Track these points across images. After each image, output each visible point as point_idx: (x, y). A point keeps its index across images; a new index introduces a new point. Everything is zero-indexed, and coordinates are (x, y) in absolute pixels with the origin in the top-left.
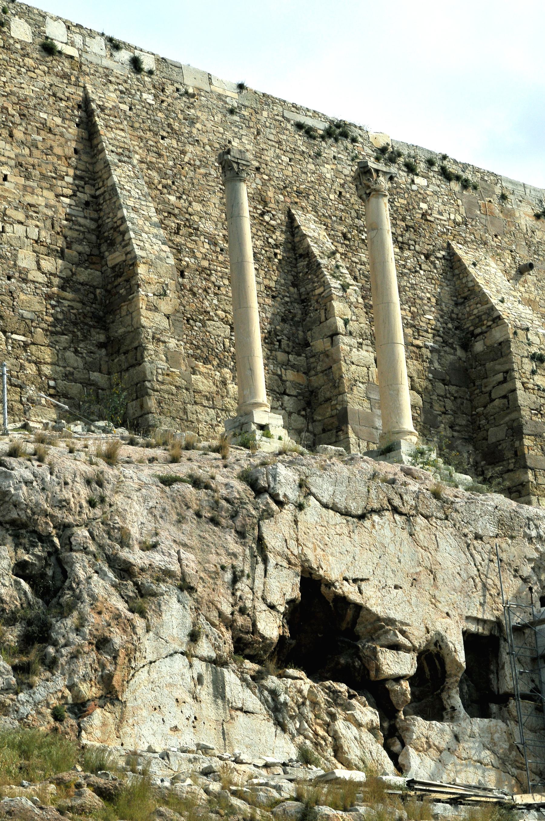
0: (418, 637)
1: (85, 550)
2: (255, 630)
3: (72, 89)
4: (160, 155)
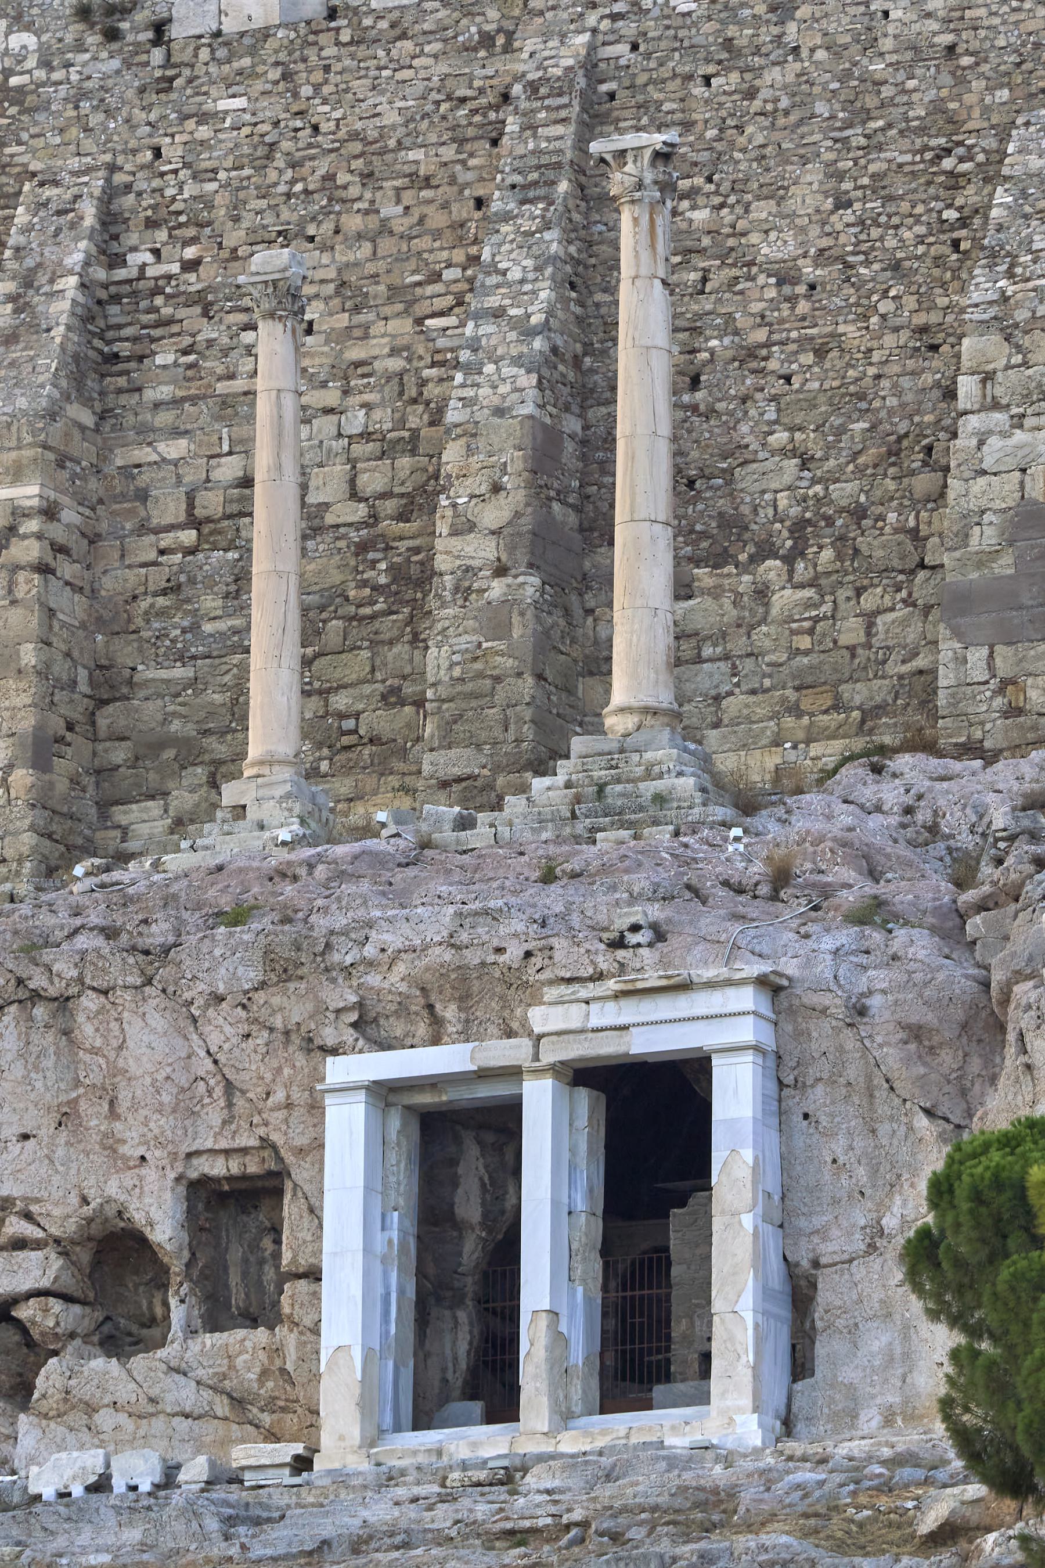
0: (62, 1216)
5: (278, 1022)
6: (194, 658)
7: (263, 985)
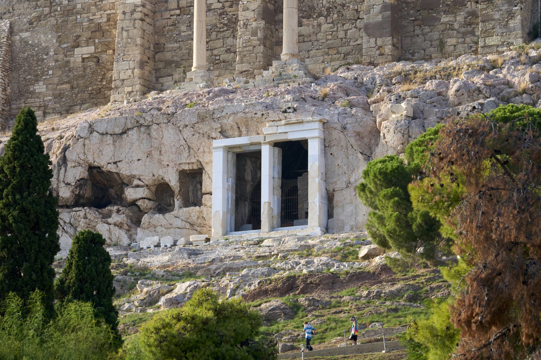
0: (148, 179)
5: (201, 131)
6: (179, 41)
7: (198, 122)
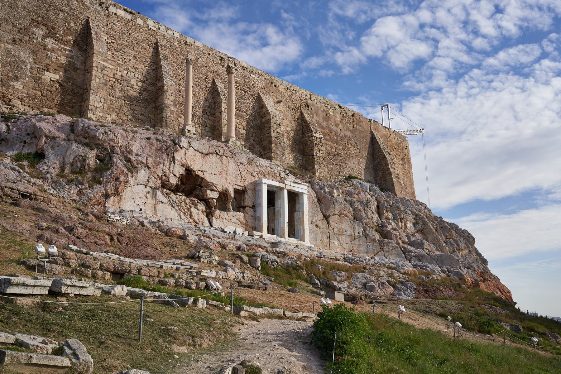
0: (220, 188)
1: (117, 154)
2: (168, 181)
3: (153, 39)
4: (177, 59)
